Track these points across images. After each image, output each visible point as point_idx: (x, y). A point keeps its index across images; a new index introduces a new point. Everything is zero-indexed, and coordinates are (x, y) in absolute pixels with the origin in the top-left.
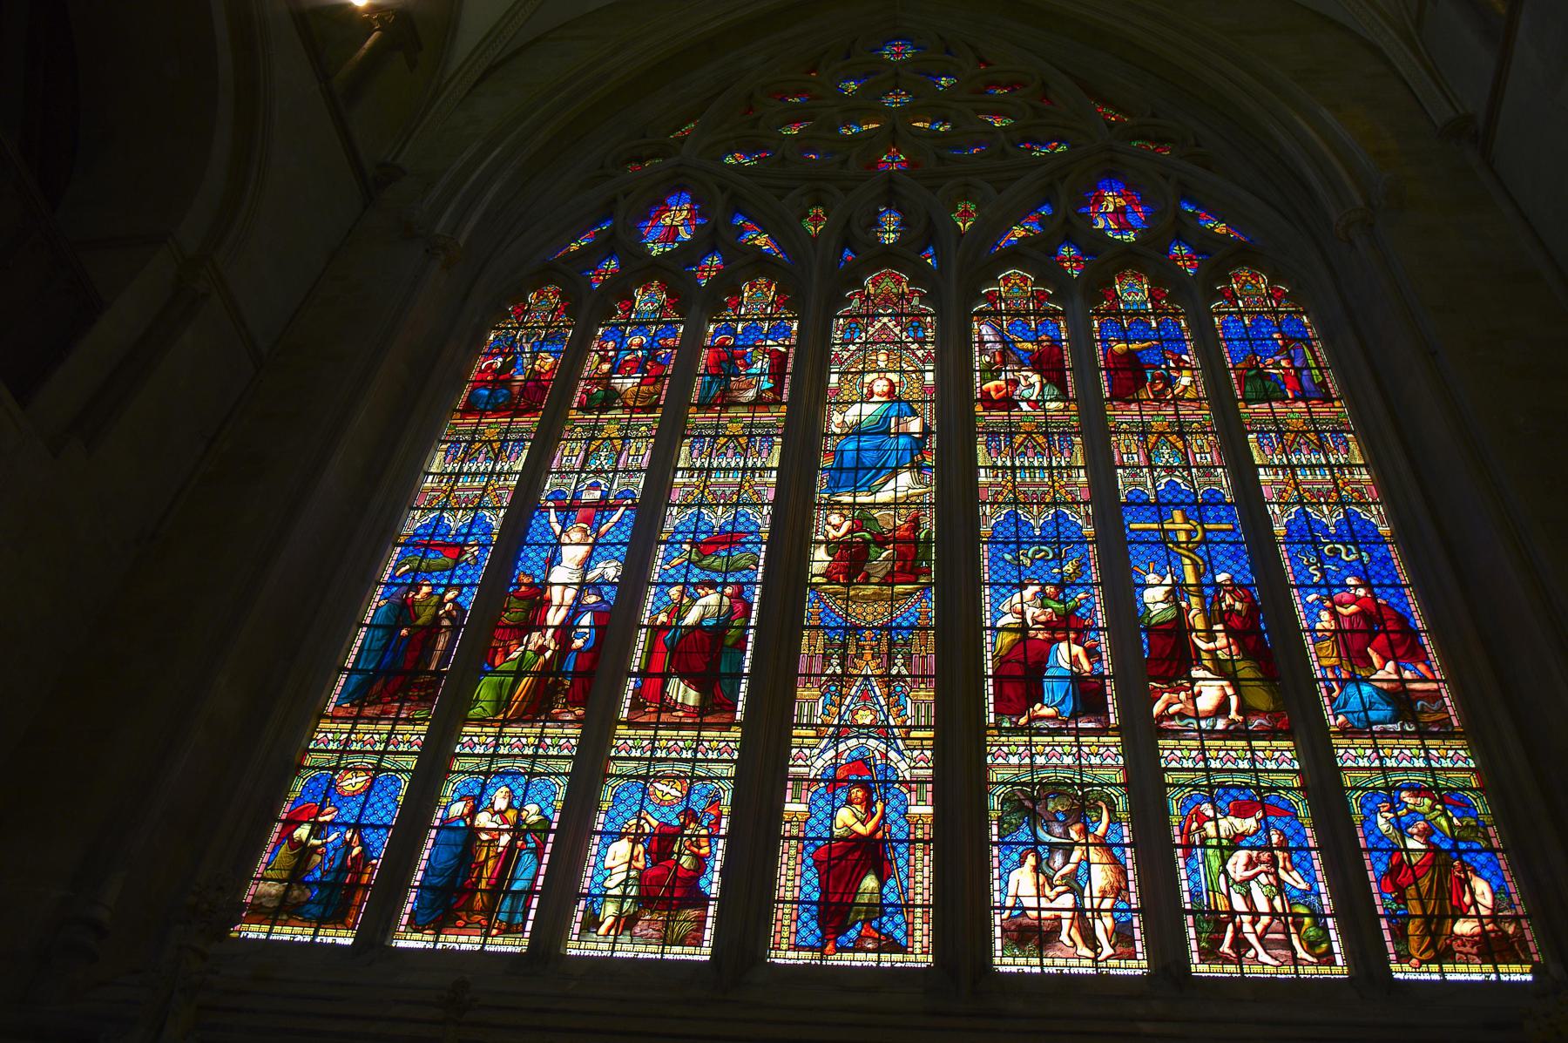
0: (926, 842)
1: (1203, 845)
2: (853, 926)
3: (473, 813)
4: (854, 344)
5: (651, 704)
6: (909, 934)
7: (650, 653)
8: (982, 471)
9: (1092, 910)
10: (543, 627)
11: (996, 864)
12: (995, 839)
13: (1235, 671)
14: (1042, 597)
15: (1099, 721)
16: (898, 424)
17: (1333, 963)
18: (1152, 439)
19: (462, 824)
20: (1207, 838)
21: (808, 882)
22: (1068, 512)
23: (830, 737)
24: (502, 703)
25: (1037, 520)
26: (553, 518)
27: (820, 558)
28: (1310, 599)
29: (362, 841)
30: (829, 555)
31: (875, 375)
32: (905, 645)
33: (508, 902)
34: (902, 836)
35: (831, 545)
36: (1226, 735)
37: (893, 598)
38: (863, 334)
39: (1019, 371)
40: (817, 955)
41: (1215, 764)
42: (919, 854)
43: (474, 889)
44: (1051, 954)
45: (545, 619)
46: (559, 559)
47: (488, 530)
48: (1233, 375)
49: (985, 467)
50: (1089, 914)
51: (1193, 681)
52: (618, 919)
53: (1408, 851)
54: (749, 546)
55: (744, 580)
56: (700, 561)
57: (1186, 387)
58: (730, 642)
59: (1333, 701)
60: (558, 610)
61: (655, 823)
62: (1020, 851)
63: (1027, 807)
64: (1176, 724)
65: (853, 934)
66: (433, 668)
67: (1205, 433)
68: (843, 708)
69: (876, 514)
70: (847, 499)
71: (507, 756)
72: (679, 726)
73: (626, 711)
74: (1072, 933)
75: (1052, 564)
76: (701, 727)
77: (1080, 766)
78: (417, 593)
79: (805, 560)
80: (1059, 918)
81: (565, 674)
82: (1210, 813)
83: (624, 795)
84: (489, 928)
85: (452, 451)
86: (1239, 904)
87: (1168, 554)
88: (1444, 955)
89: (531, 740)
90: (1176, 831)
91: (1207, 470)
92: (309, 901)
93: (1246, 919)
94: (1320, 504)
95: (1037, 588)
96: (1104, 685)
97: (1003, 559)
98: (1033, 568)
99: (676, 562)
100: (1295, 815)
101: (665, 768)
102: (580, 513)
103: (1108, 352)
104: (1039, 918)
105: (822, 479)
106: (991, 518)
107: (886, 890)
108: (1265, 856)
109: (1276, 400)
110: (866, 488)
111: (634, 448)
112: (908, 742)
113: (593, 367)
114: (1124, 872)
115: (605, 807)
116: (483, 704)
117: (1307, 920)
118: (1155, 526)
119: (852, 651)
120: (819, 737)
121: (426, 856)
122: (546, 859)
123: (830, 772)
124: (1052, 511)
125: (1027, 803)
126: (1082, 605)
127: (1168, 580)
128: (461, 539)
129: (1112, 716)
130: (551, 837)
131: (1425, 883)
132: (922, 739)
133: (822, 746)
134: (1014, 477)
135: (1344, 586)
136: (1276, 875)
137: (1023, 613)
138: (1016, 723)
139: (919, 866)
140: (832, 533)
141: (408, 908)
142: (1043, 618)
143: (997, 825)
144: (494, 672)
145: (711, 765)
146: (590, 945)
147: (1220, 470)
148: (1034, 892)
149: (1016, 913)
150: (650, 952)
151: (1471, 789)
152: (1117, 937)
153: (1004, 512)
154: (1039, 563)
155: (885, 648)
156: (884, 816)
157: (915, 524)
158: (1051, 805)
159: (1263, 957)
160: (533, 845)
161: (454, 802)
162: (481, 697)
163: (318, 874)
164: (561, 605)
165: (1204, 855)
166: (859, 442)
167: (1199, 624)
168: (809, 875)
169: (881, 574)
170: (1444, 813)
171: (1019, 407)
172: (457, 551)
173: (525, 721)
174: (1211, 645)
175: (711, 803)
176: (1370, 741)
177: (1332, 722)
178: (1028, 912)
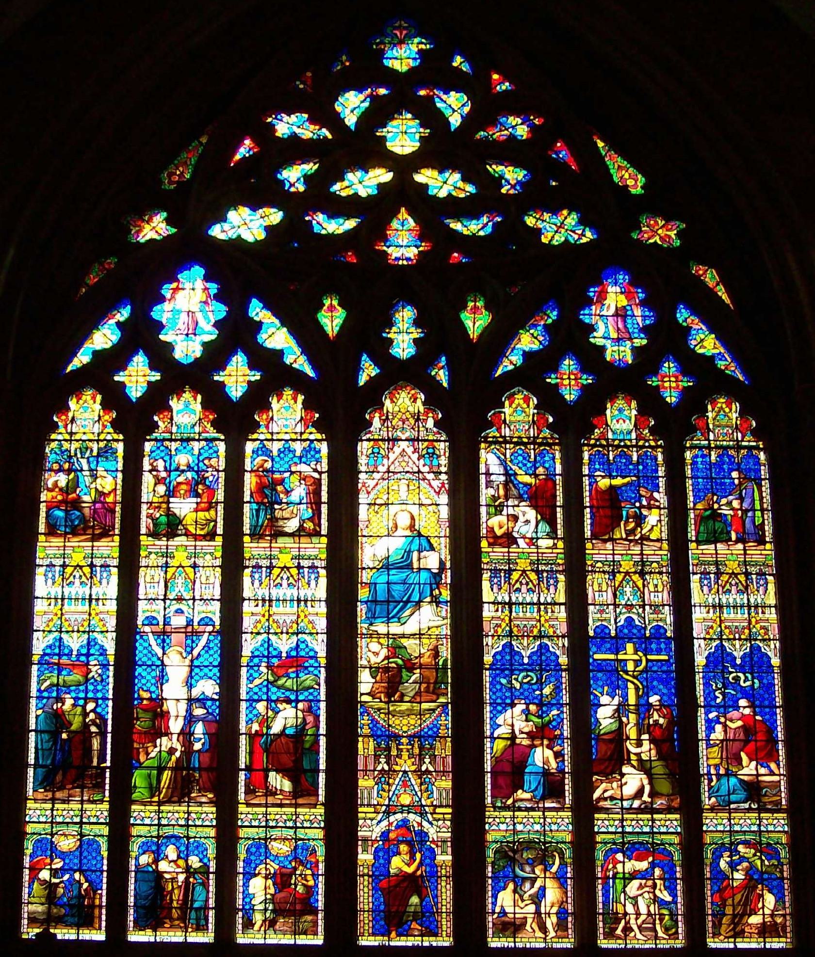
3: (156, 861)
7: (251, 753)
8: (486, 606)
10: (168, 734)
15: (559, 802)
16: (419, 559)
17: (678, 938)
18: (619, 577)
19: (150, 869)
22: (549, 644)
23: (384, 812)
24: (154, 790)
27: (366, 682)
30: (373, 677)
32: (431, 748)
35: (375, 670)
36: (639, 811)
38: (385, 461)
39: (518, 506)
40: (386, 938)
47: (103, 652)
52: (264, 921)
53: (733, 879)
55: (311, 697)
56: (276, 681)
58: (307, 745)
59: (710, 787)
61: (277, 867)
64: (607, 804)
66: (95, 763)
67: (661, 573)
68: (391, 793)
69: (405, 642)
70: (381, 628)
72: (281, 805)
75: (535, 687)
76: (296, 806)
78: (63, 704)
80: (526, 918)
81: (194, 769)
86: (630, 909)
92: (65, 915)
93: (633, 917)
94: (735, 639)
95: (524, 707)
96: (564, 778)
99: (257, 682)
105: (362, 610)
106: (492, 648)
109: (721, 542)
110: (396, 620)
112: (435, 816)
113: (151, 489)
117: (667, 917)
119: (394, 752)
124: (538, 643)
125: (511, 854)
127: (616, 701)
128: (83, 658)
130: (211, 876)
131: (738, 897)
132: (444, 814)
133: (379, 817)
134: (511, 612)
136: (654, 893)
137: (512, 725)
140: (374, 660)
142: (526, 730)
154: (526, 686)
155: (417, 751)
158: (525, 855)
159: (639, 936)
160: (200, 881)
163: (65, 899)
169: (412, 694)
170: (760, 858)
171: (517, 543)
173: (174, 802)
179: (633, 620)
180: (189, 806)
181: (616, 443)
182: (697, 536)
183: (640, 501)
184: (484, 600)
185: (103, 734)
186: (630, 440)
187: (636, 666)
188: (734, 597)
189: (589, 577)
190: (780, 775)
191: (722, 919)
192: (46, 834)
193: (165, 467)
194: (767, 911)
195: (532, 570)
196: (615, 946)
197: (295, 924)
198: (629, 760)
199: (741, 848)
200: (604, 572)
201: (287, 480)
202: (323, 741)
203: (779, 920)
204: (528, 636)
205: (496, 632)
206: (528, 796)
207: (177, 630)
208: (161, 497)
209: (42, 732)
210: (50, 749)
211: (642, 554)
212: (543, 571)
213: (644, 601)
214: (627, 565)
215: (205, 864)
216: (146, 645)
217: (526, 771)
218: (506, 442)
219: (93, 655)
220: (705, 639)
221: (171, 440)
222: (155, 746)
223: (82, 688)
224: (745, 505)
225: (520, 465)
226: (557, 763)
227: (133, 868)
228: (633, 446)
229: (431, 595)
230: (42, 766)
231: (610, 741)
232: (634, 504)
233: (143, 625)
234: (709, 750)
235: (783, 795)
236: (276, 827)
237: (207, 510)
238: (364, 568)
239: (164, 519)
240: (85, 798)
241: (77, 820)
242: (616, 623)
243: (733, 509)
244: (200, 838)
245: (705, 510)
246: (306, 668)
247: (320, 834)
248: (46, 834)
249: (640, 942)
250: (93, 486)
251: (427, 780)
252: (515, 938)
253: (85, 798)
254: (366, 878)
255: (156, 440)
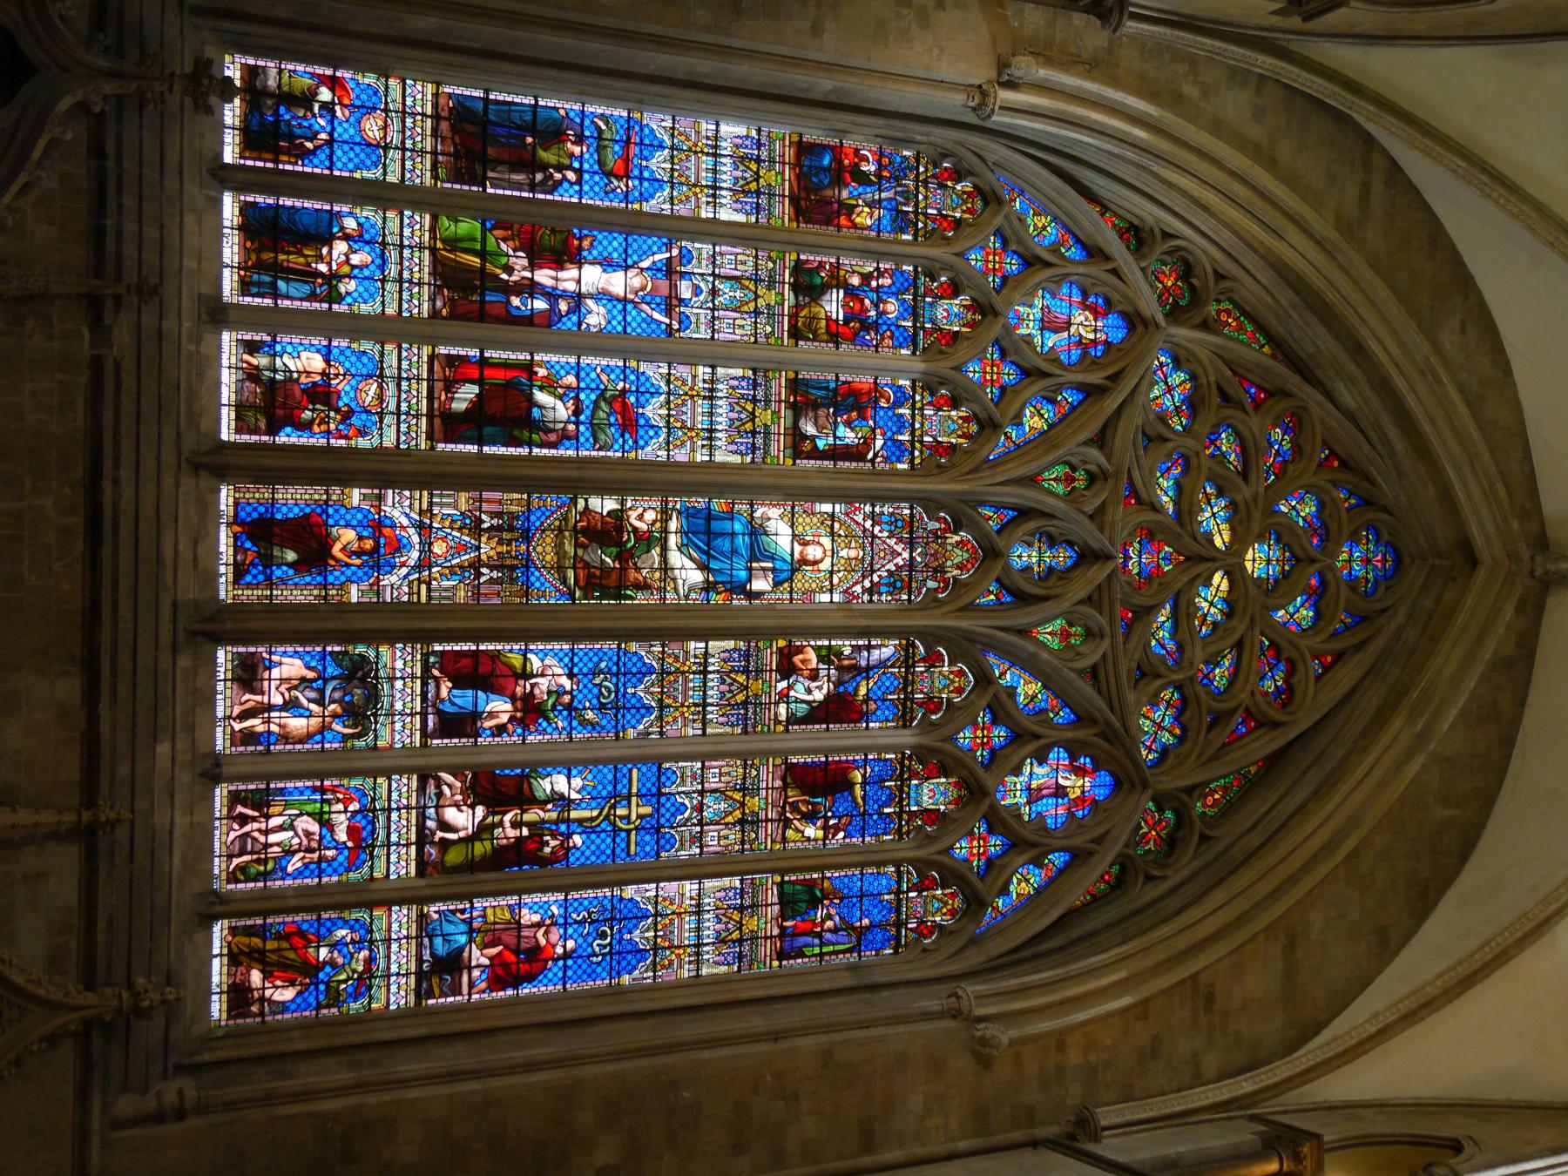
0: (325, 598)
1: (323, 801)
2: (254, 545)
3: (347, 238)
4: (873, 526)
5: (453, 372)
6: (249, 586)
7: (506, 365)
8: (702, 645)
9: (269, 717)
10: (532, 267)
11: (308, 649)
12: (329, 649)
13: (481, 840)
14: (558, 693)
15: (435, 730)
16: (764, 569)
17: (229, 882)
18: (738, 796)
19: (335, 230)
20: (330, 805)
21: (290, 510)
22: (652, 717)
23: (421, 521)
24: (453, 243)
25: (643, 691)
26: (658, 257)
27: (605, 505)
28: (554, 909)
29: (316, 148)
30: (609, 513)
31: (828, 546)
32: (511, 578)
33: (268, 279)
34: (331, 579)
35: (619, 516)
36: (421, 827)
37: (560, 569)
38: (886, 534)
39: (829, 681)
40: (231, 520)
41: (394, 816)
42: (316, 592)
43: (276, 250)
44: (235, 687)
45: (541, 268)
46: (610, 269)
47: (643, 198)
48: (815, 876)
49: (706, 648)
50: (266, 715)
51: (472, 806)
52: (257, 368)
53: (318, 947)
54: (621, 441)
55: (582, 439)
56: (605, 400)
57: (803, 832)
58: (516, 433)
59: (453, 912)
60: (552, 278)
61: (340, 387)
64: (431, 789)
65: (248, 545)
66: (490, 174)
67: (743, 842)
68: (449, 531)
69: (656, 552)
70: (673, 525)
71: (401, 257)
72: (430, 397)
73: (446, 352)
75: (595, 701)
76: (430, 416)
77: (394, 715)
78: (573, 143)
79: (603, 490)
80: (262, 693)
81: (483, 295)
82: (351, 808)
83: (365, 360)
84: (246, 269)
85: (748, 143)
86: (275, 822)
87: (604, 798)
88: (235, 958)
89: (417, 275)
90: (336, 783)
91: (699, 839)
92: (262, 115)
93: (263, 826)
94: (656, 931)
95: (568, 688)
96: (468, 736)
97: (601, 660)
98: (590, 686)
99: (604, 377)
100: (348, 870)
101: (391, 390)
102: (664, 285)
103: (853, 765)
104: (262, 680)
105: (700, 502)
106: (647, 653)
107: (285, 568)
108: (314, 845)
109: (781, 910)
110: (685, 541)
111: (744, 322)
112: (416, 583)
113: (856, 268)
114: (301, 741)
115: (355, 346)
116: (453, 227)
117: (262, 868)
118: (634, 790)
119: (506, 536)
120: (421, 512)
121: (306, 205)
122: (306, 305)
123: (388, 522)
124: (653, 704)
125: (360, 673)
126: (550, 724)
127: (574, 795)
128: (636, 172)
129: (439, 741)
130: (325, 306)
131: (292, 955)
132: (419, 593)
133: (412, 515)
134: (694, 673)
135: (565, 938)
136: (299, 850)
137: (543, 675)
138: (433, 667)
139: (305, 592)
140: (633, 515)
141: (260, 199)
142: (537, 691)
144: (484, 230)
145: (394, 428)
146: (234, 349)
147: (698, 851)
148: (284, 676)
149: (267, 663)
150: (227, 394)
151: (370, 1003)
153: (654, 663)
154: (596, 691)
155: (508, 562)
156: (348, 565)
157: (643, 586)
158: (358, 691)
159: (232, 835)
160: (318, 291)
161: (356, 218)
162: (460, 224)
163: (287, 117)
164: (557, 279)
165: (315, 801)
166: (744, 534)
167: (526, 817)
168: (296, 510)
169: (586, 558)
170: (349, 978)
171: (782, 679)
172: (621, 172)
173: (434, 267)
174: (507, 824)
175: (359, 430)
176: (414, 934)
177: (432, 909)
179: (682, 814)
180: (429, 284)
181: (906, 789)
182: (790, 882)
183: (833, 817)
184: (710, 643)
185: (533, 187)
186: (908, 805)
187: (621, 818)
188: (710, 927)
189: (739, 762)
190: (470, 995)
191: (258, 936)
192: (387, 103)
193: (883, 286)
194: (268, 993)
195: (748, 697)
196: (218, 805)
197: (254, 407)
198: (494, 814)
199: (364, 954)
200: (744, 778)
201: (864, 423)
202: (524, 451)
203: (254, 1009)
204: (662, 693)
205: (669, 656)
206: (444, 693)
207: (673, 287)
208: (846, 280)
209: (535, 113)
210: (510, 121)
211: (767, 820)
212: (747, 709)
213: (707, 824)
214: (754, 803)
215: (343, 299)
216: (655, 249)
217: (480, 693)
218: (907, 668)
219: (641, 184)
220: (657, 896)
221: (915, 295)
222: (515, 251)
223: (596, 167)
224: (828, 935)
225: (879, 683)
226: (490, 728)
227: (336, 208)
228: (901, 807)
229: (717, 583)
230: (486, 108)
231: (521, 790)
232: (830, 810)
233: (681, 248)
234: (506, 908)
235: (441, 1000)
236: (399, 390)
237: (828, 331)
238: (752, 505)
239: (818, 281)
240: (440, 158)
241: (409, 144)
242: (679, 793)
243: (823, 922)
244: (383, 296)
245: (822, 891)
246: (622, 436)
247: (389, 441)
248: (387, 103)
249: (224, 837)
250: (860, 202)
251: (467, 574)
252: (232, 680)
253: (440, 158)
254: (325, 497)
255: (916, 278)
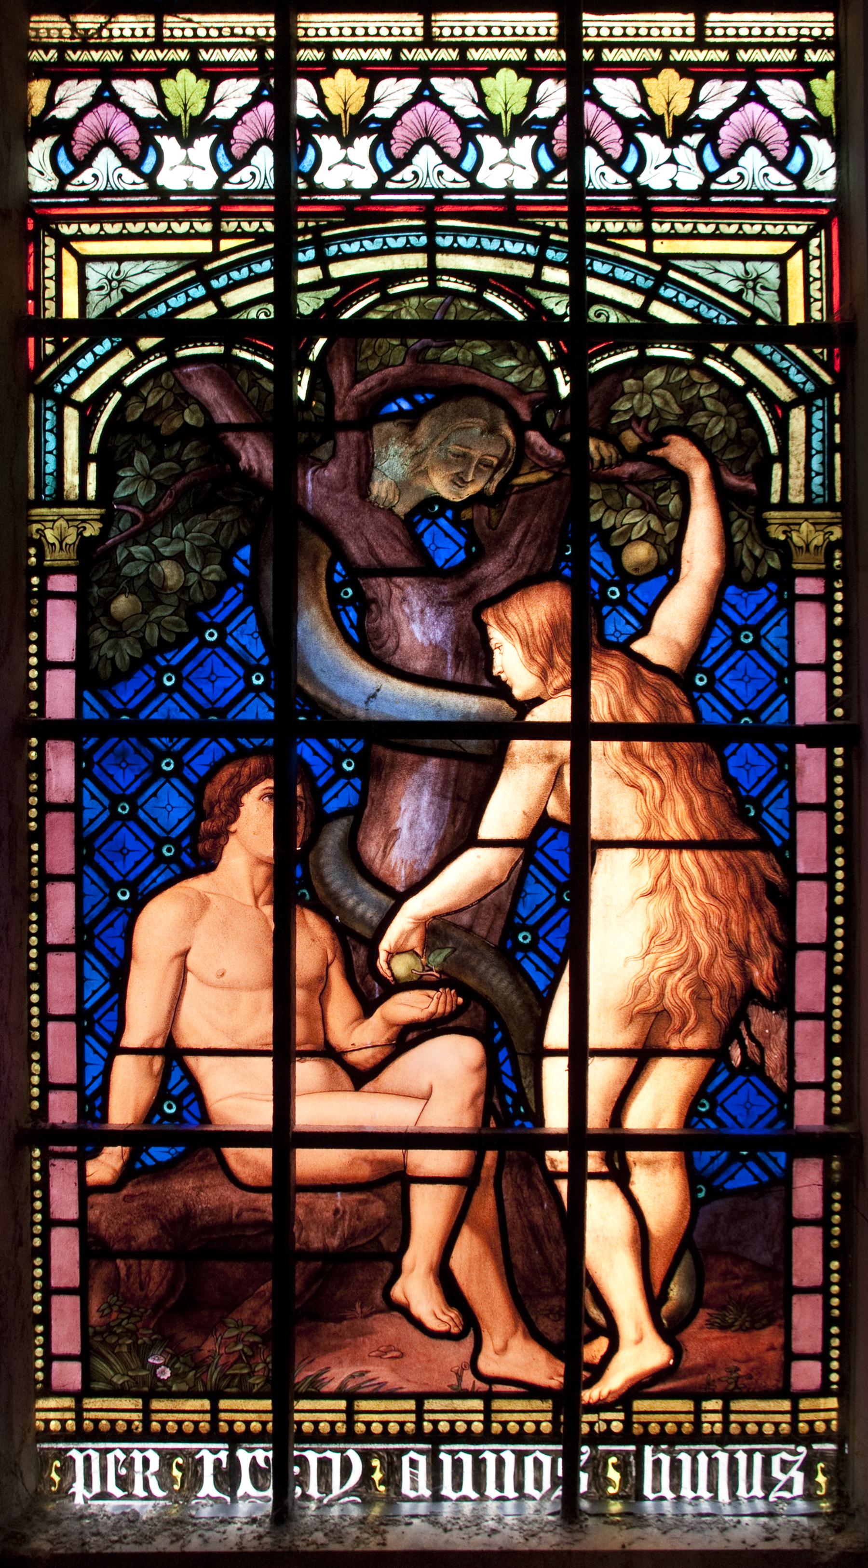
62: (201, 766)
63: (248, 478)
74: (459, 1261)
143: (78, 597)
152: (698, 1279)
178: (230, 1153)
